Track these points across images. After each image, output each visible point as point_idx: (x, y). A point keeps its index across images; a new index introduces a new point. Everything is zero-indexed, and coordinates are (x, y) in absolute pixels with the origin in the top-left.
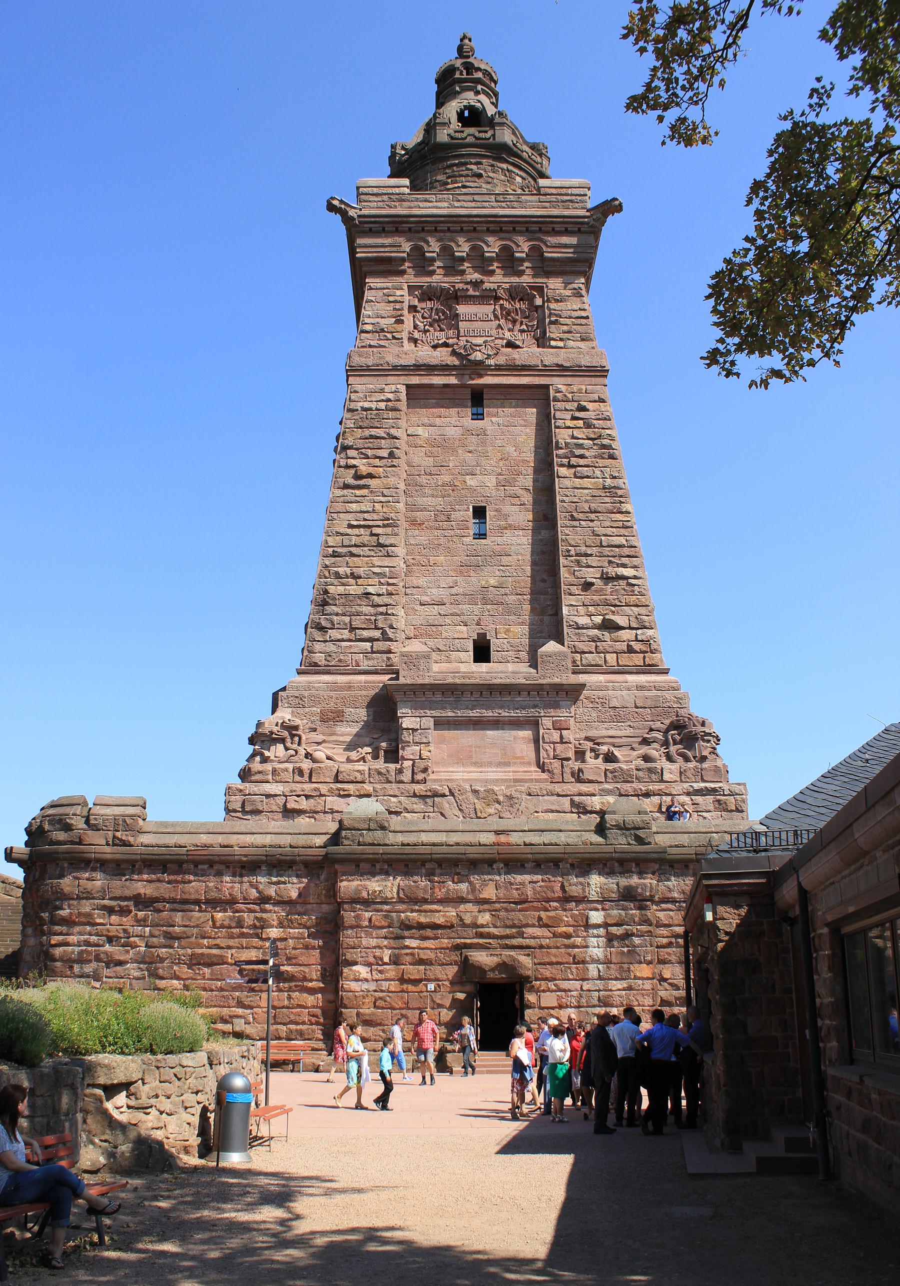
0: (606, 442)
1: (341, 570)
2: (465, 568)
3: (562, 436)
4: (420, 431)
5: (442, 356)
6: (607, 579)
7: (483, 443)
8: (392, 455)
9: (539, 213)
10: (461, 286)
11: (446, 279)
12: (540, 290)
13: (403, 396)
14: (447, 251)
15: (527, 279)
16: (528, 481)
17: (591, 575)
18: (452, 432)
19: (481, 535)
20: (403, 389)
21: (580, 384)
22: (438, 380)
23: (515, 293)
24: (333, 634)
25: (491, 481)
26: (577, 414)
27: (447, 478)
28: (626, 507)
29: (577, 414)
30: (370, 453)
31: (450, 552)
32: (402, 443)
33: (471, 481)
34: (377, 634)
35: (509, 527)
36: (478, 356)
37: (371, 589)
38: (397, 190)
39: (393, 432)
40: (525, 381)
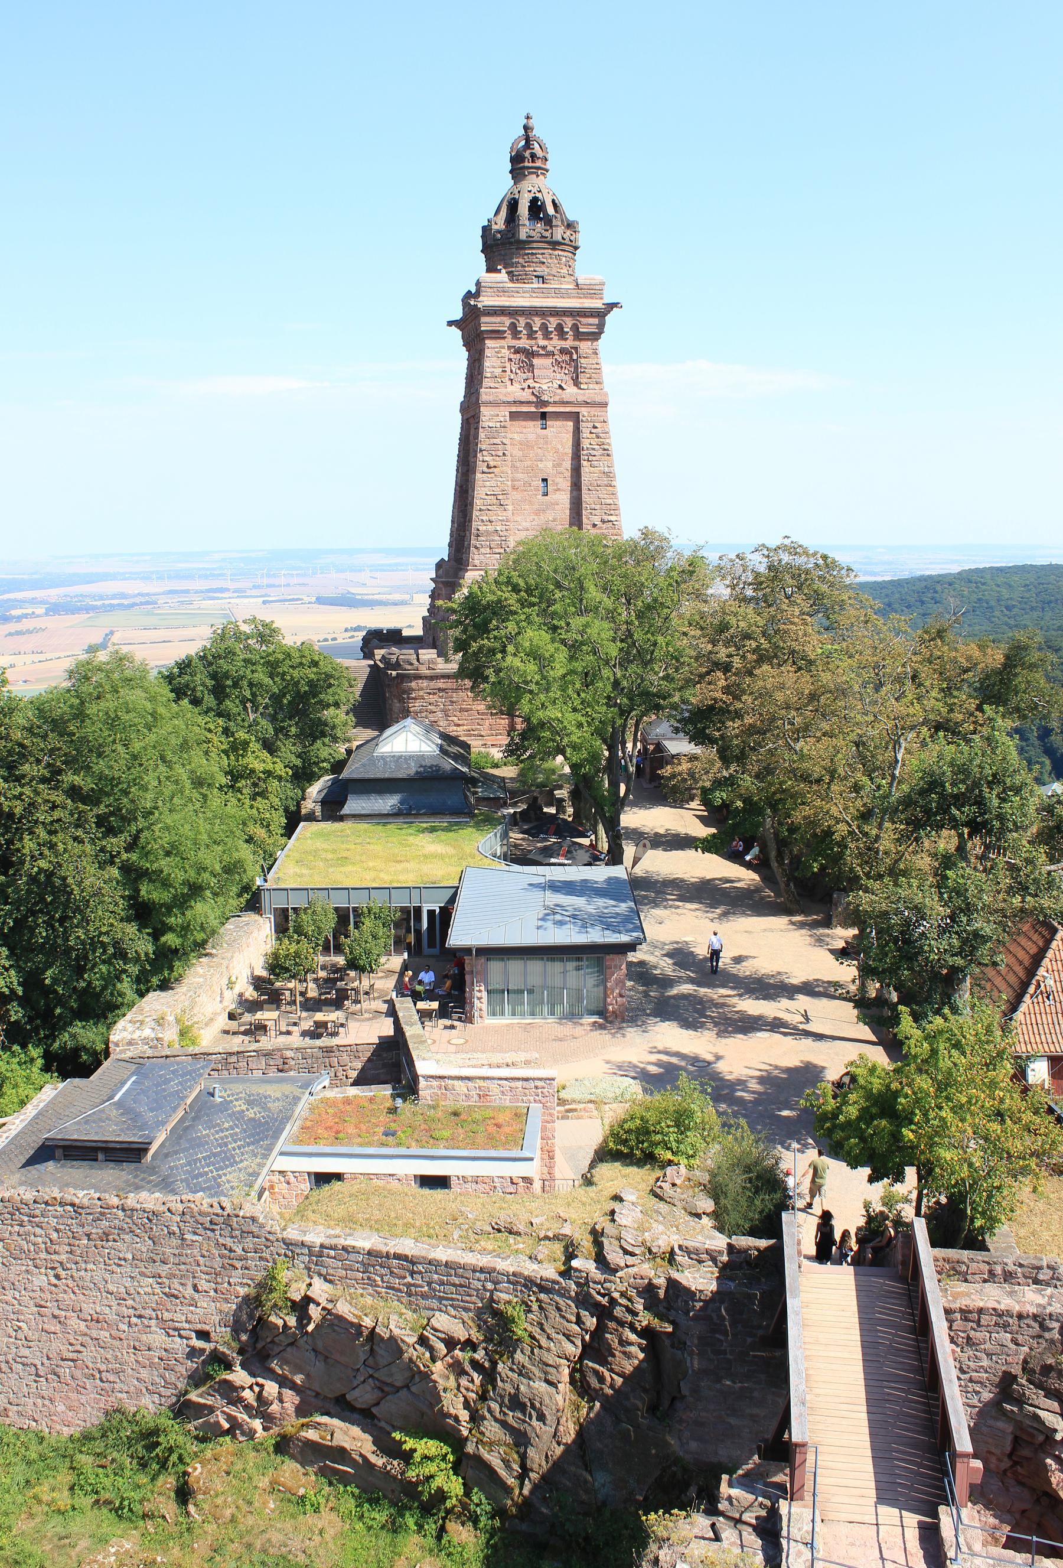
0: (606, 447)
1: (485, 518)
2: (538, 512)
3: (585, 443)
4: (516, 436)
5: (526, 396)
6: (603, 522)
7: (546, 443)
8: (504, 454)
9: (578, 305)
10: (535, 348)
11: (528, 342)
12: (576, 349)
13: (508, 418)
14: (529, 326)
15: (568, 344)
16: (568, 464)
17: (597, 520)
18: (531, 437)
19: (546, 494)
20: (508, 414)
21: (594, 411)
22: (525, 409)
23: (563, 351)
24: (482, 550)
25: (550, 464)
26: (594, 431)
27: (529, 463)
28: (613, 483)
29: (594, 431)
30: (493, 453)
31: (531, 503)
32: (508, 447)
33: (541, 465)
34: (502, 551)
35: (559, 490)
36: (545, 398)
37: (498, 528)
38: (501, 285)
39: (504, 441)
40: (568, 409)
